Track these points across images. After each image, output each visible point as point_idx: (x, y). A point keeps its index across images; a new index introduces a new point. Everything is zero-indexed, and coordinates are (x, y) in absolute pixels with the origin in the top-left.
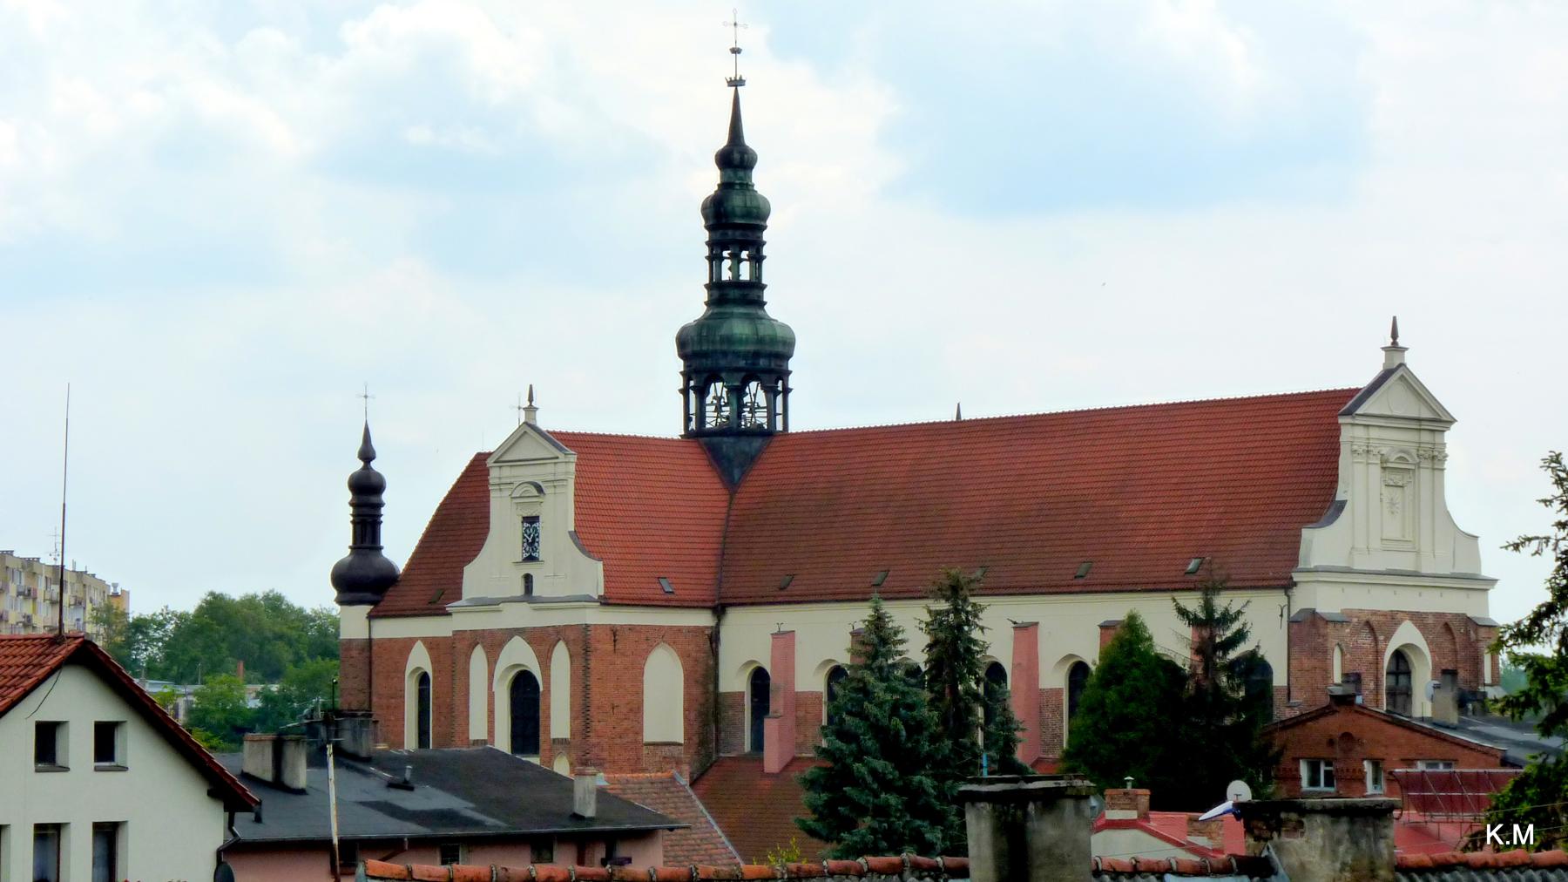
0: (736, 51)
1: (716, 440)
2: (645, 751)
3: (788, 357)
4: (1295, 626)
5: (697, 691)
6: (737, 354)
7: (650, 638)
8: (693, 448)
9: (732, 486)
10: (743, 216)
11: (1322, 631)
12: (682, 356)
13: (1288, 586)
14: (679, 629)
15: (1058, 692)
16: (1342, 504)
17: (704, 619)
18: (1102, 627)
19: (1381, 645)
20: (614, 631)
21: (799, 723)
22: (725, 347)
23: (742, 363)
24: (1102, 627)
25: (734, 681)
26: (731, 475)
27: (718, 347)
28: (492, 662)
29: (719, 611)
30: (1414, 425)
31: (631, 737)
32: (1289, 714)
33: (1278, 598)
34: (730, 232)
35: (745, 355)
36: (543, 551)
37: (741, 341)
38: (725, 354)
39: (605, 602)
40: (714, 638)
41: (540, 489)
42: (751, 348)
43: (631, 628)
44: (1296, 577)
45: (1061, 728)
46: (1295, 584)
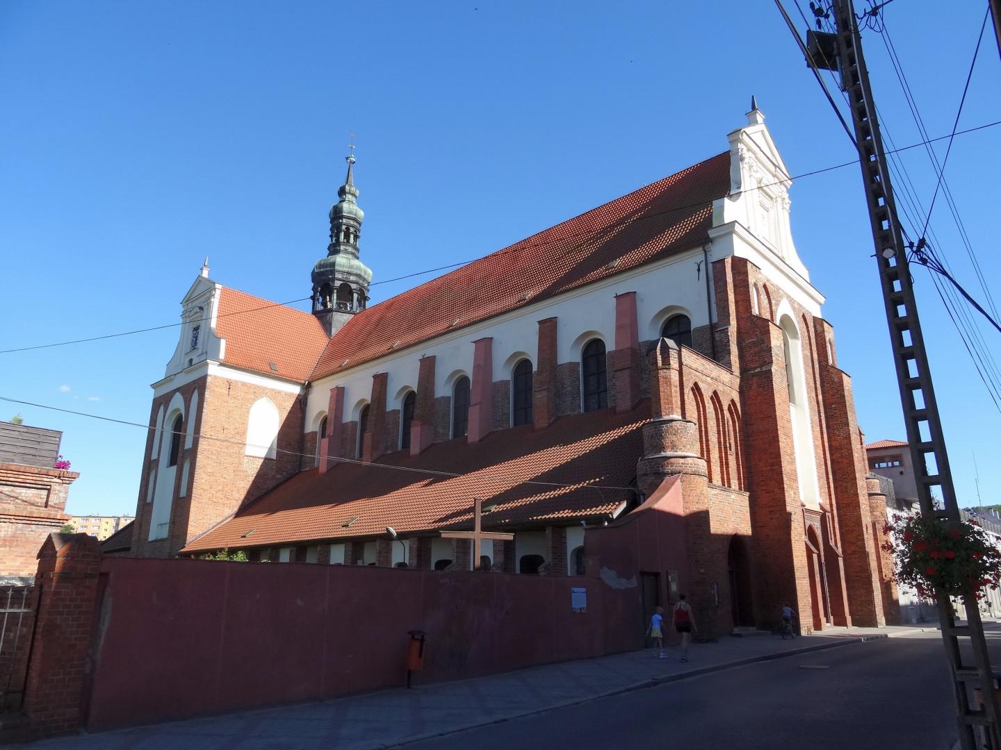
2: (246, 460)
4: (718, 265)
7: (258, 392)
10: (348, 213)
12: (313, 282)
15: (505, 383)
18: (540, 322)
24: (540, 322)
25: (312, 426)
28: (165, 412)
30: (772, 168)
33: (696, 256)
35: (343, 272)
37: (340, 265)
41: (201, 308)
42: (346, 270)
43: (244, 384)
44: (712, 233)
45: (509, 408)
46: (710, 241)
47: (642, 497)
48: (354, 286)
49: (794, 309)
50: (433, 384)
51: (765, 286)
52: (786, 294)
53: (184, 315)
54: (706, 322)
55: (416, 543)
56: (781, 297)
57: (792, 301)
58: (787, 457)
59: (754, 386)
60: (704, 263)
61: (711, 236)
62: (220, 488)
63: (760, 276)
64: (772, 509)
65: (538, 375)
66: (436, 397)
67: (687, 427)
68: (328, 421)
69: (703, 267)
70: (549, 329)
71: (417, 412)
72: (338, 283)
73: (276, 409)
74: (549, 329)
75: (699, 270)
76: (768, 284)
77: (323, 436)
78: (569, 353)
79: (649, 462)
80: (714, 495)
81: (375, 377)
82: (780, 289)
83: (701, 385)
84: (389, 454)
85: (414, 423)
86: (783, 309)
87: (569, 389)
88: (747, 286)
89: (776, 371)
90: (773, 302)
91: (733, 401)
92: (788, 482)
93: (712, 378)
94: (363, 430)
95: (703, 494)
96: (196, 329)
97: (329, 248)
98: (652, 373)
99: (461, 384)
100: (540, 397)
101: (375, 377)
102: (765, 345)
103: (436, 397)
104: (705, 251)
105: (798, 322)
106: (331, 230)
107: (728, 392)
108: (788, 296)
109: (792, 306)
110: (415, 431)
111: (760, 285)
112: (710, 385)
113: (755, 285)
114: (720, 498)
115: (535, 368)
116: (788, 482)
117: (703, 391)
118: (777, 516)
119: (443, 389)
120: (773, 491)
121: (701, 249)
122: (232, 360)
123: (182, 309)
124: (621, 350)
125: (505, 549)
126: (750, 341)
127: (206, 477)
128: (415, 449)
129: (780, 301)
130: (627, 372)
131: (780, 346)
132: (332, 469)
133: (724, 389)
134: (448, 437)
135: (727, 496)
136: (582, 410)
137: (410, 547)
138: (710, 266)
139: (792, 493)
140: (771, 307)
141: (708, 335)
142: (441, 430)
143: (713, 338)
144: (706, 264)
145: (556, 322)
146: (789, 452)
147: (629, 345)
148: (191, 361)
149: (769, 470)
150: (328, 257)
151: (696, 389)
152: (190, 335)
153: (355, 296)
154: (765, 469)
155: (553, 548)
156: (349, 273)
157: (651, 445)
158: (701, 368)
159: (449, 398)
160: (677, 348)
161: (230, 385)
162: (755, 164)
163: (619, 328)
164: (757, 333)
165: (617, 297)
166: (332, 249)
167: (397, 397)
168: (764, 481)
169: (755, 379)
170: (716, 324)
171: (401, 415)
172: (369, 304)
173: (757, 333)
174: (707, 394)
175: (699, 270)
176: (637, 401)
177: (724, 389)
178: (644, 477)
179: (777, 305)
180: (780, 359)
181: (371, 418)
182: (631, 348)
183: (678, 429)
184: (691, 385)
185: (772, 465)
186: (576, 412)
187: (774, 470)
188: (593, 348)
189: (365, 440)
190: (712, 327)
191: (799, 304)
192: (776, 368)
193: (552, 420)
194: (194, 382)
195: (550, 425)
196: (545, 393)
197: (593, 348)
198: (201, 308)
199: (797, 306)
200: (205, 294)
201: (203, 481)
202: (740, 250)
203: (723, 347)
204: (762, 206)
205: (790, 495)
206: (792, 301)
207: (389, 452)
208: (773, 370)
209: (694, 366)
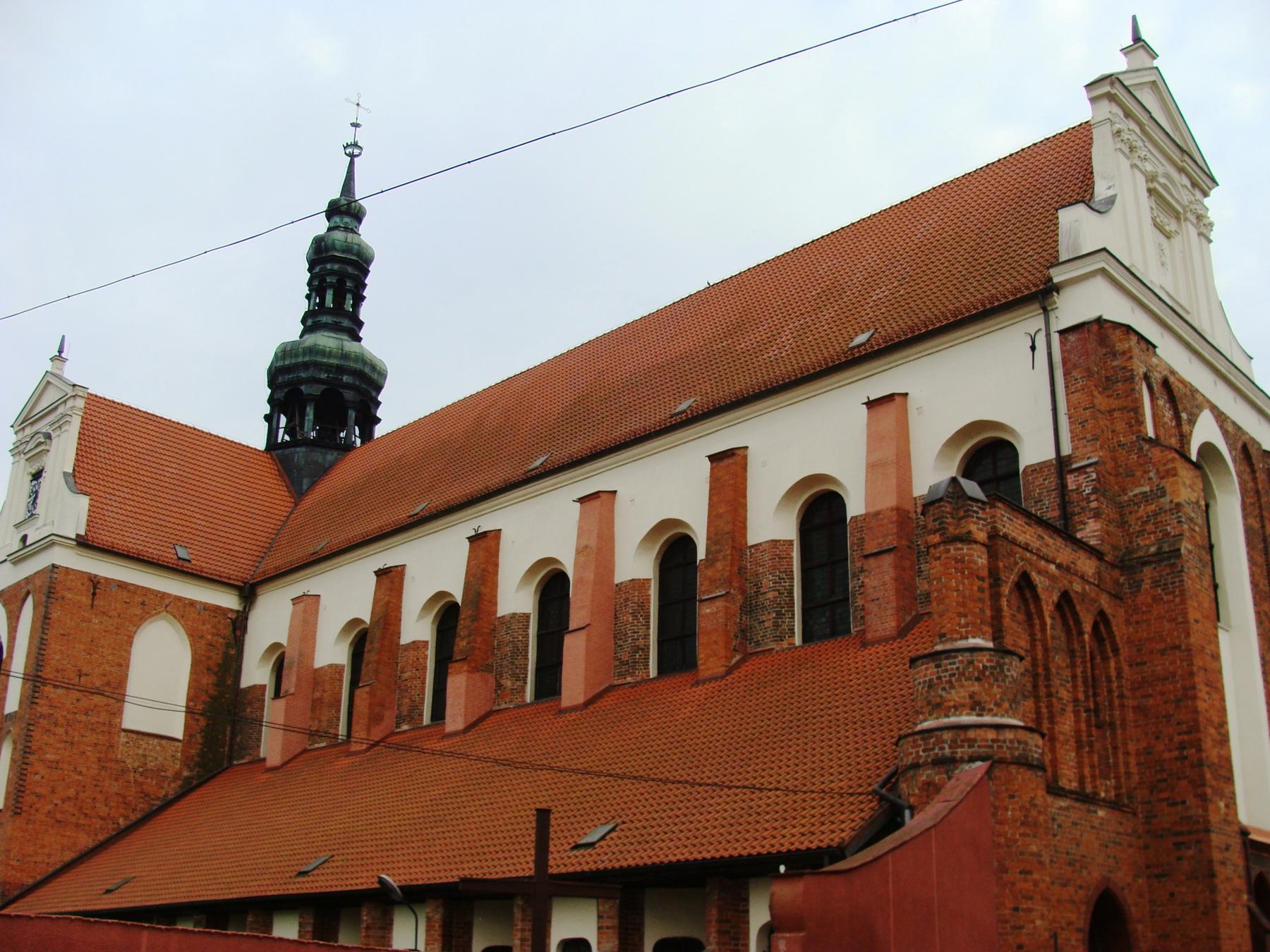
0: (356, 125)
1: (287, 451)
2: (123, 738)
3: (379, 388)
5: (208, 680)
6: (319, 366)
7: (151, 604)
8: (266, 458)
9: (298, 494)
10: (343, 252)
11: (1120, 347)
12: (271, 384)
13: (1043, 295)
14: (192, 603)
15: (641, 584)
16: (1111, 201)
17: (229, 601)
18: (713, 458)
19: (1185, 428)
20: (95, 582)
21: (316, 704)
22: (307, 359)
23: (324, 376)
24: (713, 458)
25: (256, 673)
26: (301, 484)
27: (300, 360)
29: (249, 593)
30: (1175, 154)
31: (103, 717)
32: (1056, 513)
33: (1032, 322)
34: (329, 266)
35: (328, 368)
36: (40, 509)
38: (306, 366)
39: (83, 543)
40: (239, 623)
41: (48, 436)
43: (122, 585)
44: (1058, 276)
45: (647, 636)
46: (1057, 288)
47: (907, 813)
48: (348, 395)
49: (1225, 433)
50: (495, 586)
51: (1166, 383)
52: (1208, 401)
53: (16, 451)
54: (1050, 454)
55: (441, 910)
56: (1200, 408)
57: (1221, 418)
58: (1212, 731)
59: (1146, 585)
60: (1043, 333)
61: (1056, 280)
62: (72, 792)
63: (1154, 360)
64: (1180, 839)
65: (707, 567)
66: (499, 614)
67: (1005, 663)
68: (286, 661)
69: (1041, 342)
70: (729, 469)
71: (461, 644)
72: (316, 390)
73: (185, 637)
74: (729, 469)
75: (1033, 348)
76: (1172, 379)
77: (277, 695)
78: (771, 522)
79: (923, 739)
80: (1061, 808)
81: (380, 573)
82: (1197, 391)
83: (1036, 578)
84: (405, 732)
85: (453, 668)
86: (1205, 431)
87: (770, 595)
88: (1131, 379)
89: (1190, 552)
90: (1184, 416)
91: (1102, 613)
92: (1214, 783)
93: (1059, 566)
94: (354, 683)
95: (1036, 806)
96: (37, 476)
97: (304, 321)
98: (932, 550)
99: (553, 586)
100: (711, 615)
101: (380, 573)
102: (1168, 499)
103: (499, 614)
104: (1046, 311)
105: (1234, 461)
106: (309, 284)
107: (1093, 595)
108: (1214, 409)
109: (1221, 427)
110: (457, 683)
111: (1156, 377)
112: (1052, 577)
113: (1146, 377)
114: (1074, 815)
115: (701, 554)
116: (1214, 783)
117: (1039, 590)
118: (1190, 853)
119: (516, 598)
120: (1184, 802)
121: (1037, 306)
122: (105, 538)
123: (14, 438)
124: (877, 514)
125: (621, 923)
126: (1137, 491)
127: (43, 771)
128: (455, 720)
129: (1197, 416)
130: (888, 560)
131: (1197, 502)
132: (290, 761)
133: (1084, 589)
134: (523, 697)
135: (1089, 811)
136: (798, 640)
137: (429, 919)
138: (1056, 338)
139: (1222, 804)
140: (1179, 424)
141: (1052, 482)
142: (508, 683)
143: (1063, 486)
144: (1048, 335)
145: (745, 457)
146: (1216, 720)
147: (890, 501)
148: (24, 538)
149: (1176, 759)
150: (301, 337)
151: (1025, 585)
152: (26, 485)
153: (352, 414)
154: (1166, 755)
155: (719, 921)
156: (340, 370)
157: (929, 703)
158: (1035, 544)
159: (527, 616)
160: (985, 499)
161: (95, 588)
162: (1139, 144)
163: (873, 467)
164: (1152, 474)
165: (870, 404)
166: (309, 322)
167: (421, 617)
168: (1165, 780)
169: (1147, 570)
170: (1069, 456)
171: (431, 653)
172: (379, 431)
173: (1152, 474)
174: (1049, 600)
175: (1033, 348)
176: (908, 618)
177: (1084, 589)
178: (912, 772)
179: (1192, 422)
180: (1197, 528)
181: (370, 657)
182: (898, 509)
183: (985, 667)
184: (1013, 577)
185: (1182, 747)
186: (785, 645)
187: (1186, 758)
188: (820, 507)
189: (357, 702)
190: (1062, 465)
191: (1234, 423)
192: (1190, 547)
193: (734, 661)
194: (28, 580)
195: (730, 671)
196: (720, 604)
197: (820, 507)
198: (48, 436)
199: (1230, 429)
200: (56, 408)
201: (38, 777)
202: (1118, 310)
203: (1084, 504)
204: (1158, 226)
205: (1218, 808)
206: (1221, 418)
207: (405, 727)
208: (1183, 551)
209: (1021, 539)
